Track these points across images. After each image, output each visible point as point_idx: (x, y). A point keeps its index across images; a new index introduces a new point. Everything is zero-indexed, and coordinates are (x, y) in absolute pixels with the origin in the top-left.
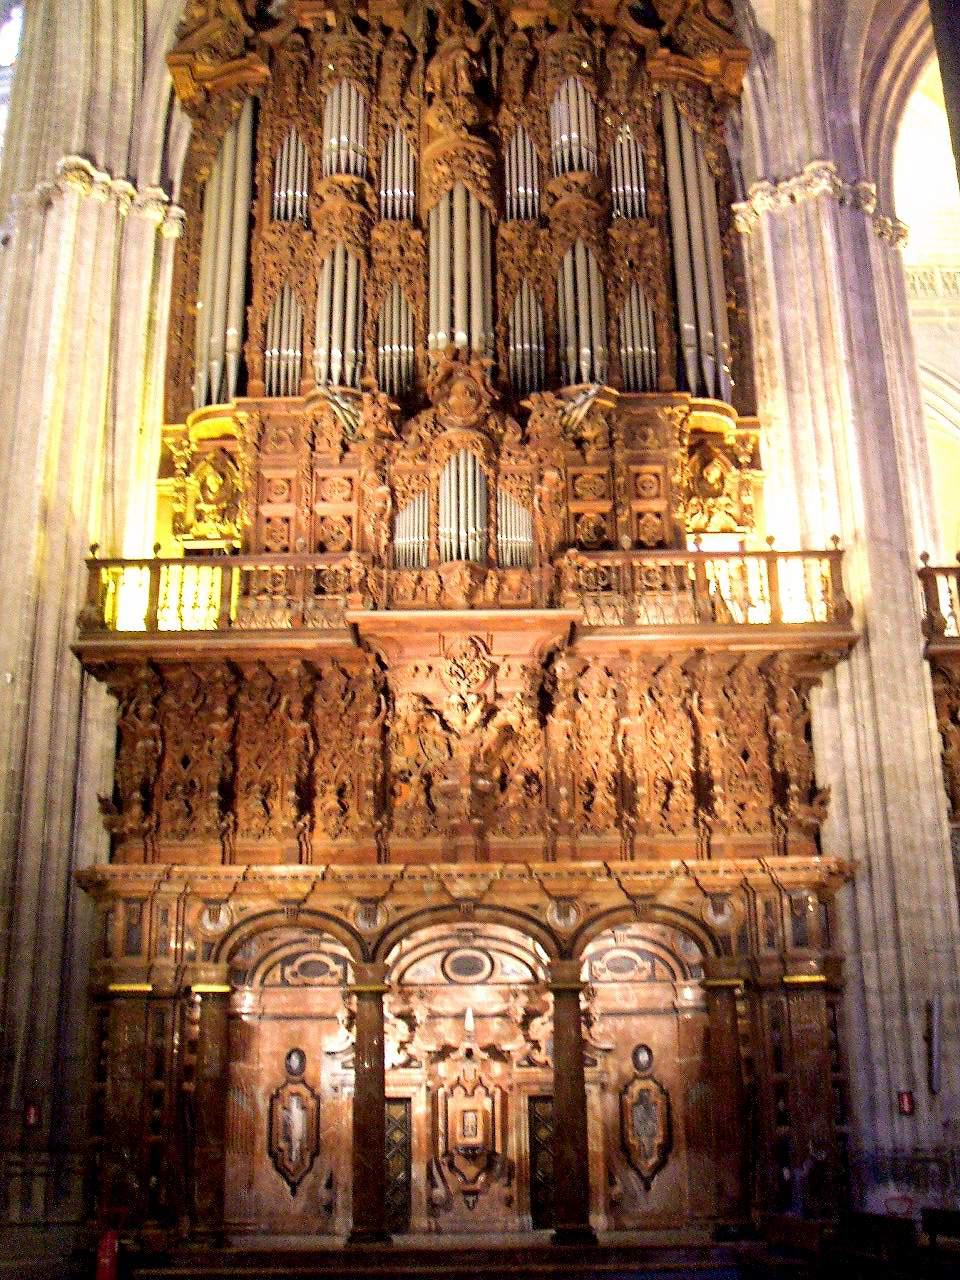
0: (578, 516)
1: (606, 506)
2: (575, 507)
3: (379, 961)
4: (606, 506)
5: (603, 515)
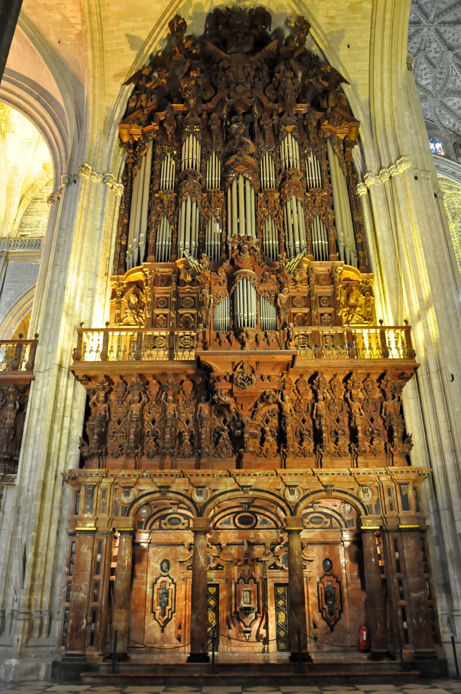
0: (295, 314)
1: (306, 310)
2: (294, 311)
3: (205, 516)
4: (306, 310)
5: (305, 314)
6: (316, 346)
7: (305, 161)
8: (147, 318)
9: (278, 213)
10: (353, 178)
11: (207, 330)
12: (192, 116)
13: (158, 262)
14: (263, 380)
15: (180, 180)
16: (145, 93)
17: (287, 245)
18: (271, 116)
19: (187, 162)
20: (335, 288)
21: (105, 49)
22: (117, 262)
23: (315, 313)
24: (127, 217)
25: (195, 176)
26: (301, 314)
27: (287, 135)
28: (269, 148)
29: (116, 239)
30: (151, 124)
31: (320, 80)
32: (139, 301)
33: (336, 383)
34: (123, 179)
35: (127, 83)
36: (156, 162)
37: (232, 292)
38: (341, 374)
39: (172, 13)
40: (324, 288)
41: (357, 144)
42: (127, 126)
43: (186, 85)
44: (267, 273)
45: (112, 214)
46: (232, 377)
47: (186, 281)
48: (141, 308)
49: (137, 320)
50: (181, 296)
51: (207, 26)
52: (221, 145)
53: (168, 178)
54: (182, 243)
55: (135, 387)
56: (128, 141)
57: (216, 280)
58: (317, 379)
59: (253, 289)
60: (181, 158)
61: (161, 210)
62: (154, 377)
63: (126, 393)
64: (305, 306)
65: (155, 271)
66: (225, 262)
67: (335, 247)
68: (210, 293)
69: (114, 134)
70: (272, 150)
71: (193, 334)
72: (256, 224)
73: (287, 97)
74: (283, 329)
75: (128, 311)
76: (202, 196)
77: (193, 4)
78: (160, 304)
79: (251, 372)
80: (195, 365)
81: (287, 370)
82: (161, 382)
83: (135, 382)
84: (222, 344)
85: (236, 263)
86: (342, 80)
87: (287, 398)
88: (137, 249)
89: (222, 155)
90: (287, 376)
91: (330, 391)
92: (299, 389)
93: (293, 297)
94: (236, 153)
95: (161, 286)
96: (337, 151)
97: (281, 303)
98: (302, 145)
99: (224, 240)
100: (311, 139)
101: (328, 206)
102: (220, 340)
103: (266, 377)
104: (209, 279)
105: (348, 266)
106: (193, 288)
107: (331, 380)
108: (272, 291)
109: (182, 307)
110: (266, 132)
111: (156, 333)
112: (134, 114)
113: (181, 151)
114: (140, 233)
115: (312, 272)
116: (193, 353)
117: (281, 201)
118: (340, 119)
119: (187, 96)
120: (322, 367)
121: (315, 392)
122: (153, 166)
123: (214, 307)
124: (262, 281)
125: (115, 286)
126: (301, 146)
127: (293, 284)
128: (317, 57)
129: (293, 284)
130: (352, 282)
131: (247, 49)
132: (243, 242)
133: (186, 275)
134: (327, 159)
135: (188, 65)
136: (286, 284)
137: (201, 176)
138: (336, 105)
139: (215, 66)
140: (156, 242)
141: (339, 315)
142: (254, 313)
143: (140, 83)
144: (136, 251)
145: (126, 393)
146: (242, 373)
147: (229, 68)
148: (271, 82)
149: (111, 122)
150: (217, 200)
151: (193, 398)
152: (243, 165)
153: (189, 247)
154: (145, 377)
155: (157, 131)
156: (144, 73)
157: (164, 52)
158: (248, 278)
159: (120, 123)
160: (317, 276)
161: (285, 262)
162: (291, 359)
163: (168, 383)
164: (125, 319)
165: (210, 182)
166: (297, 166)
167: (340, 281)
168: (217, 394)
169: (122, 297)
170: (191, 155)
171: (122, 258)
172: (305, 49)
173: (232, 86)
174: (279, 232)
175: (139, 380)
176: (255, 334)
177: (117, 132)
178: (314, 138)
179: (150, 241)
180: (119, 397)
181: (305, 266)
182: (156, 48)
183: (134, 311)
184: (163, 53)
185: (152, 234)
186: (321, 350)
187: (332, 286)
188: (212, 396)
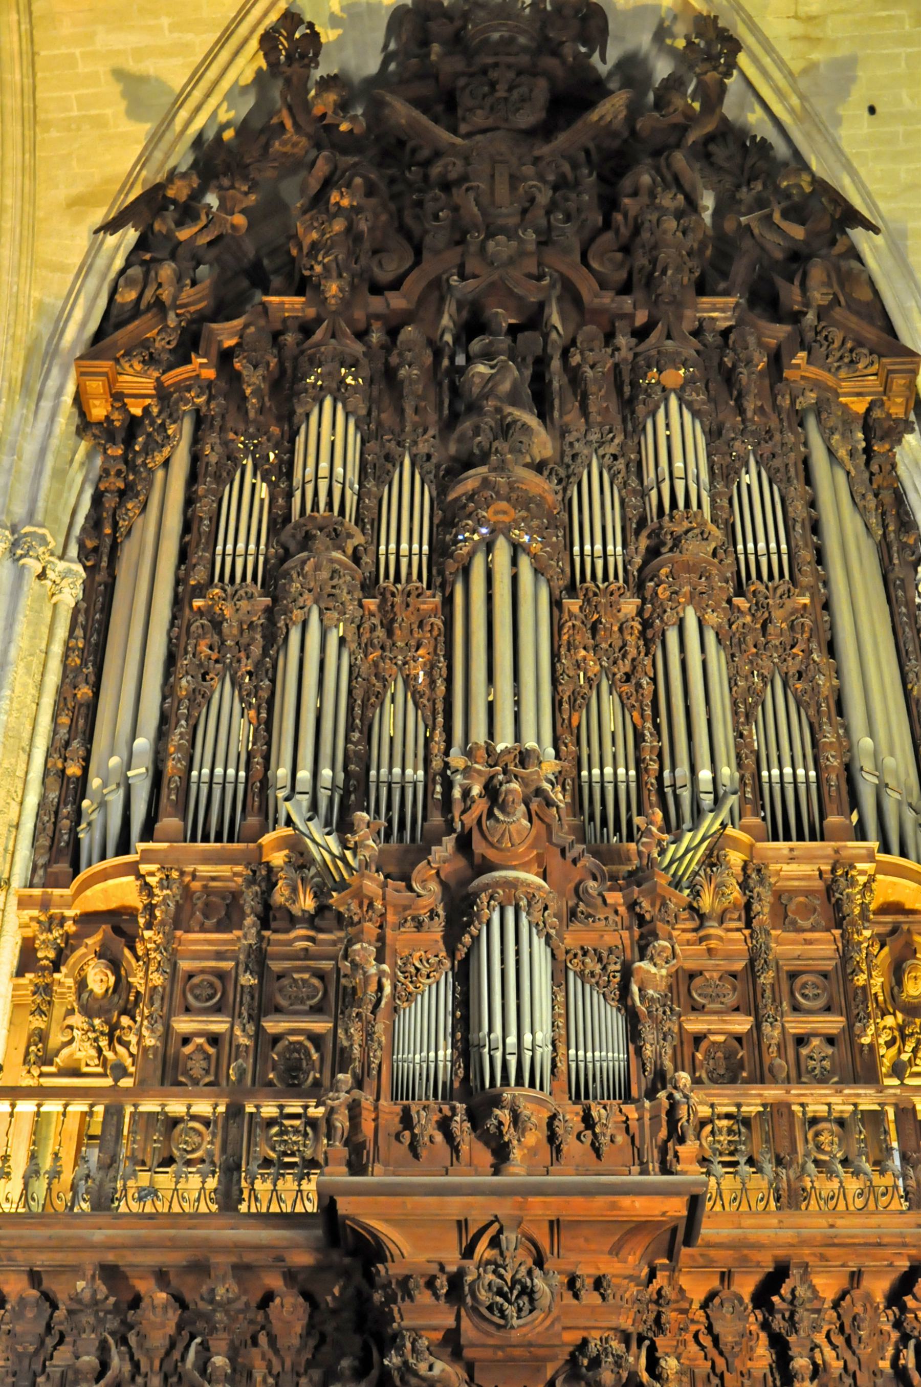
0: (698, 1039)
1: (742, 1024)
2: (694, 1025)
4: (742, 1024)
5: (739, 1039)
6: (779, 1162)
7: (728, 486)
8: (146, 1050)
9: (634, 668)
10: (904, 546)
11: (366, 1099)
12: (333, 336)
13: (194, 839)
14: (576, 1296)
15: (286, 550)
16: (173, 257)
17: (667, 781)
18: (609, 337)
19: (310, 489)
20: (846, 940)
21: (41, 116)
22: (44, 841)
23: (776, 1033)
24: (92, 679)
25: (337, 537)
26: (721, 1038)
27: (666, 400)
28: (601, 444)
29: (48, 755)
30: (188, 361)
31: (777, 217)
32: (121, 985)
33: (859, 1309)
35: (111, 226)
36: (201, 489)
37: (461, 954)
38: (878, 1273)
40: (808, 942)
41: (912, 431)
42: (106, 365)
43: (315, 235)
44: (591, 884)
45: (36, 668)
46: (456, 1281)
47: (296, 910)
48: (125, 1012)
49: (109, 1055)
50: (276, 966)
52: (431, 432)
53: (241, 546)
54: (283, 772)
55: (87, 1319)
56: (107, 417)
57: (406, 908)
58: (785, 1290)
59: (539, 944)
60: (290, 475)
61: (215, 656)
62: (161, 1276)
63: (50, 1342)
64: (737, 1009)
65: (182, 873)
66: (439, 843)
67: (844, 788)
68: (380, 959)
69: (60, 392)
70: (612, 449)
71: (317, 1112)
72: (556, 705)
73: (664, 272)
74: (651, 1094)
75: (78, 1020)
76: (361, 605)
78: (197, 997)
79: (530, 1262)
80: (319, 1232)
81: (671, 1254)
82: (188, 1297)
83: (87, 1296)
84: (423, 1153)
85: (479, 846)
86: (852, 217)
87: (670, 1365)
88: (121, 792)
89: (438, 467)
90: (670, 1279)
91: (839, 1340)
92: (717, 1329)
93: (692, 976)
94: (484, 459)
95: (203, 930)
96: (842, 453)
97: (642, 997)
98: (720, 434)
99: (437, 764)
100: (749, 414)
101: (814, 645)
102: (414, 1136)
103: (589, 1282)
104: (378, 905)
105: (894, 859)
106: (322, 936)
107: (842, 1297)
108: (610, 952)
109: (278, 1010)
110: (592, 388)
111: (176, 1108)
112: (131, 327)
113: (292, 451)
114: (134, 737)
115: (761, 882)
116: (310, 1186)
117: (646, 624)
118: (849, 345)
119: (318, 269)
120: (804, 1243)
121: (779, 1344)
122: (189, 501)
123: (396, 1010)
124: (573, 914)
125: (35, 925)
126: (713, 434)
127: (690, 925)
128: (764, 146)
129: (690, 925)
130: (911, 918)
131: (527, 118)
132: (505, 772)
133: (294, 890)
134: (809, 480)
135: (322, 168)
136: (661, 927)
137: (359, 539)
138: (836, 301)
139: (414, 174)
140: (190, 769)
141: (866, 1040)
142: (543, 1034)
143: (157, 226)
144: (116, 800)
145: (50, 1342)
146: (497, 1267)
147: (464, 178)
148: (607, 224)
149: (52, 353)
150: (414, 619)
151: (310, 1364)
152: (508, 500)
153: (308, 787)
154: (126, 1278)
155: (210, 384)
156: (171, 193)
157: (243, 128)
158: (523, 903)
159: (81, 358)
160: (778, 895)
161: (659, 843)
162: (685, 1213)
163: (212, 1301)
164: (65, 1052)
165: (392, 558)
166: (700, 506)
167: (864, 916)
168: (400, 1349)
169: (57, 970)
170: (324, 465)
171: (66, 823)
172: (724, 120)
173: (475, 238)
174: (639, 737)
175: (103, 1290)
176: (545, 1115)
177: (71, 388)
178: (761, 410)
179: (170, 764)
180: (20, 1356)
181: (735, 858)
182: (214, 114)
183: (97, 1022)
184: (238, 133)
185: (176, 739)
186: (799, 1178)
187: (837, 932)
188: (383, 1356)
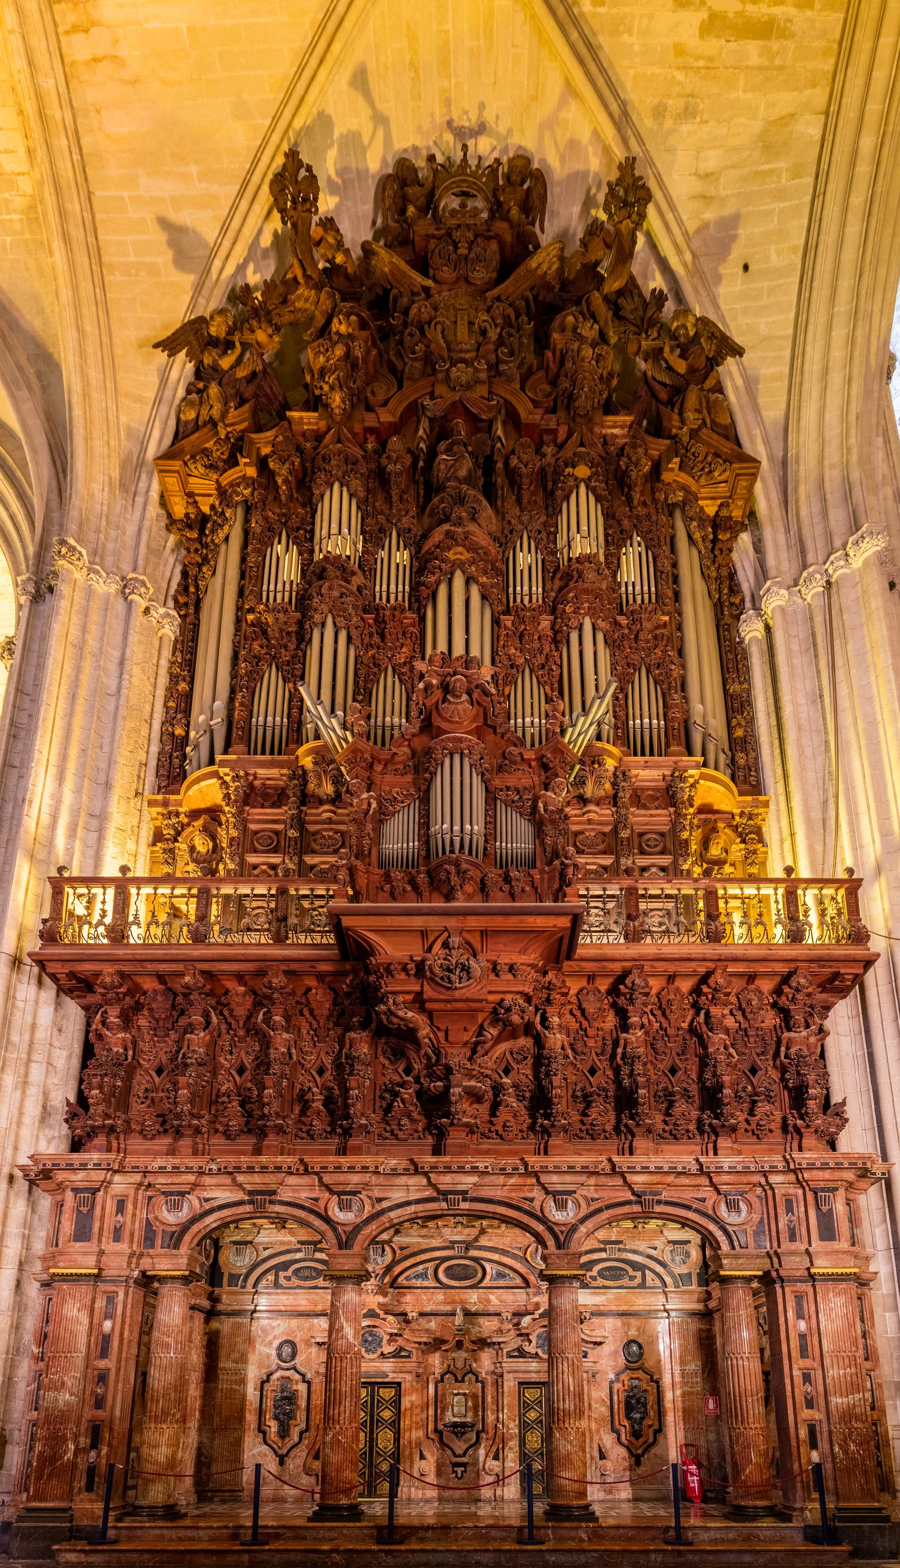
12: (339, 441)
34: (176, 601)
39: (278, 147)
51: (379, 221)
77: (336, 135)
159: (159, 458)
